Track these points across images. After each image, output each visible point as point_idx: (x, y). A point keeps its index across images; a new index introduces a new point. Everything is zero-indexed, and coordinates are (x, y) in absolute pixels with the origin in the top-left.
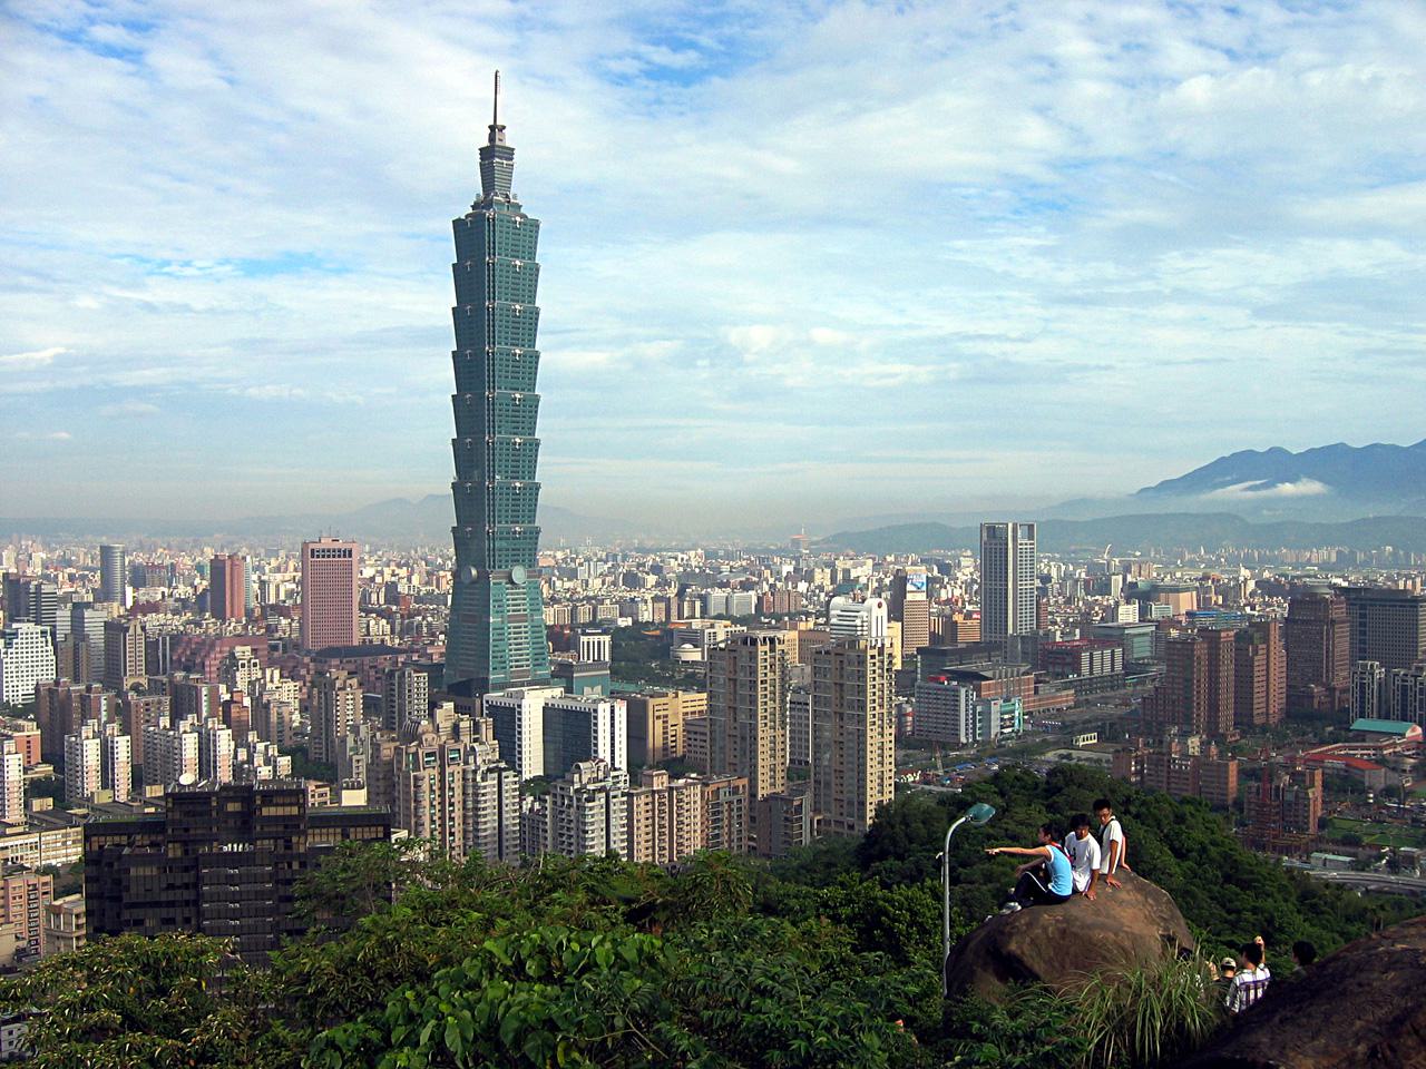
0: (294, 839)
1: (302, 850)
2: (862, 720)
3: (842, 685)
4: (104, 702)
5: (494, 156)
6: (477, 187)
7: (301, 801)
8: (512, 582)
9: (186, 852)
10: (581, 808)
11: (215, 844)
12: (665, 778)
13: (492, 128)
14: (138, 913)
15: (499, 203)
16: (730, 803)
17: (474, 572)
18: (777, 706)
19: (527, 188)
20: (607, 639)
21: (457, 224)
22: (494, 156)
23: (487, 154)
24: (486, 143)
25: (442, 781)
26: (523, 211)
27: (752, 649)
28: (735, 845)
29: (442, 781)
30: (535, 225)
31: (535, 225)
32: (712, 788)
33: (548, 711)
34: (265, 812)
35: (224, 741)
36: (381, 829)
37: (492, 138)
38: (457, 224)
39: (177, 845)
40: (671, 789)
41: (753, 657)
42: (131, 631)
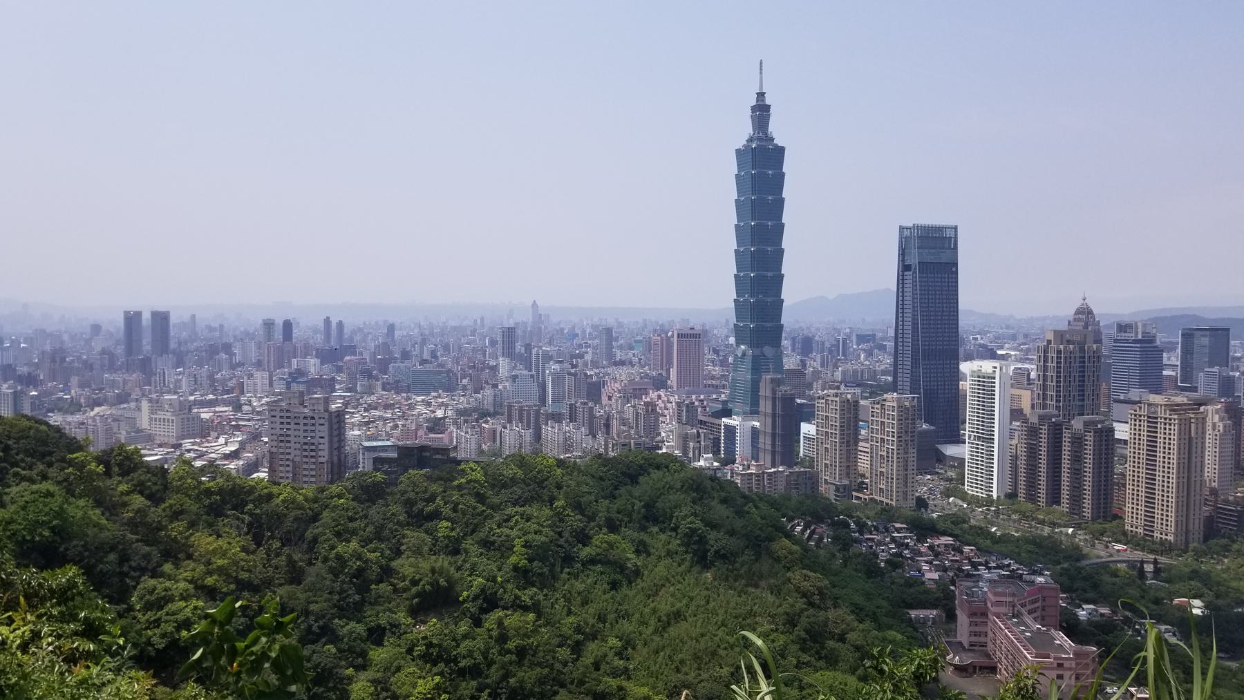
5: (761, 112)
19: (779, 131)
21: (738, 151)
22: (761, 112)
30: (781, 150)
31: (781, 150)
38: (738, 151)
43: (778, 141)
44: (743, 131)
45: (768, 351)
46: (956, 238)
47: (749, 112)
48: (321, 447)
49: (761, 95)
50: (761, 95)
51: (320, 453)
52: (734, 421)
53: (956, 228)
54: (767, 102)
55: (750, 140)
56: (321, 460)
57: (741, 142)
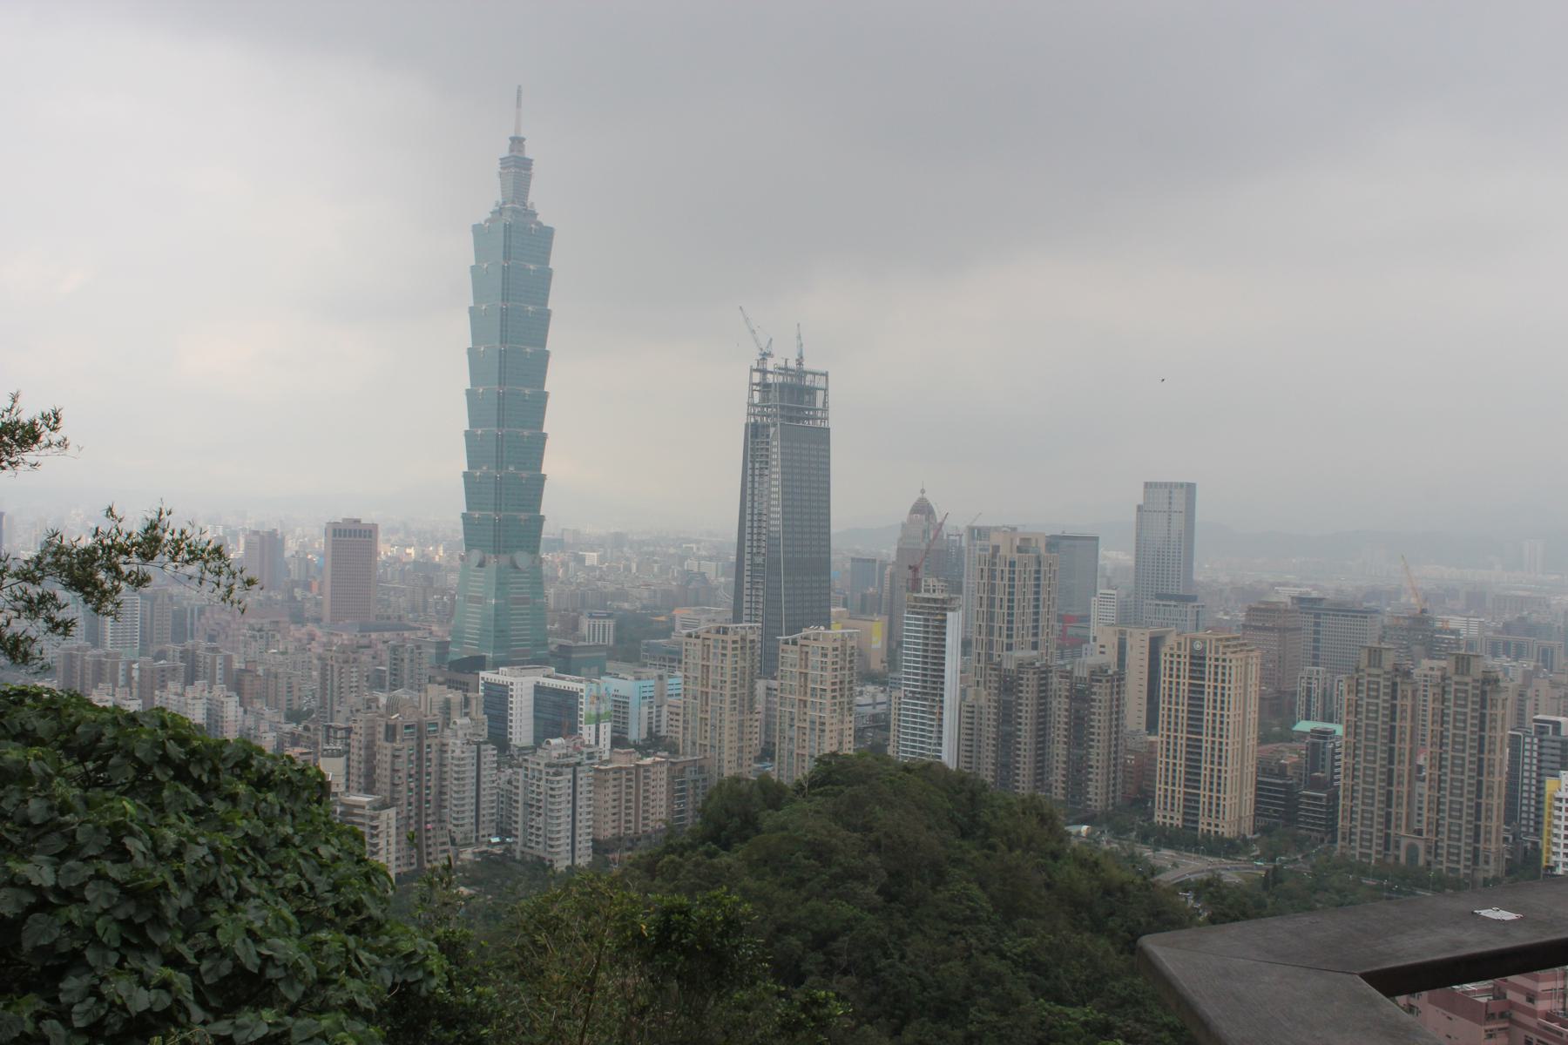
4: (121, 667)
5: (517, 168)
16: (695, 781)
18: (746, 691)
19: (545, 202)
20: (611, 623)
21: (477, 229)
24: (506, 153)
25: (420, 751)
26: (539, 218)
29: (420, 751)
31: (547, 234)
33: (539, 689)
35: (232, 709)
37: (511, 150)
38: (477, 229)
43: (545, 218)
44: (486, 197)
45: (522, 559)
46: (826, 390)
47: (497, 166)
49: (517, 142)
50: (517, 142)
52: (502, 676)
53: (826, 375)
54: (528, 154)
55: (500, 211)
57: (483, 214)
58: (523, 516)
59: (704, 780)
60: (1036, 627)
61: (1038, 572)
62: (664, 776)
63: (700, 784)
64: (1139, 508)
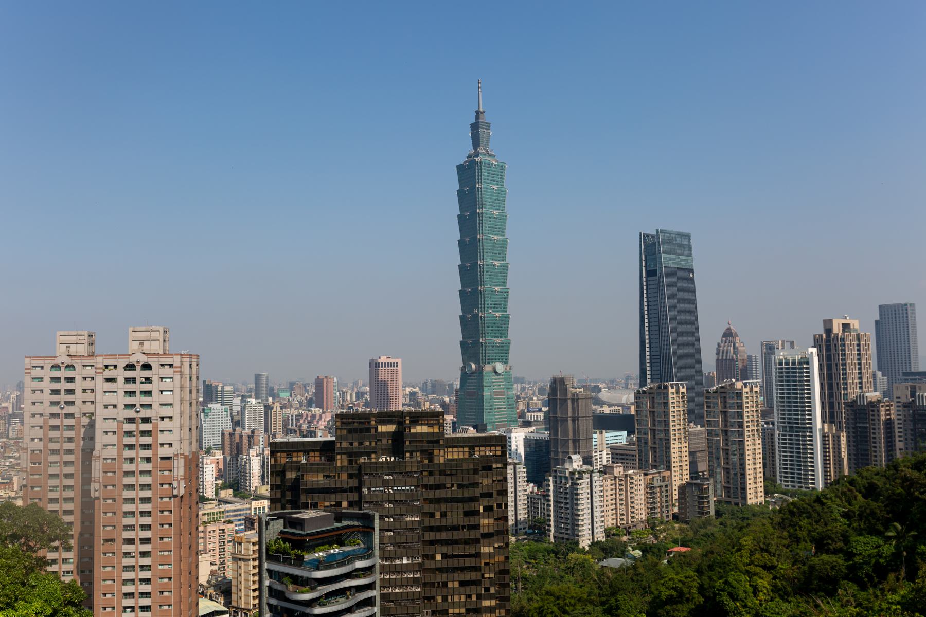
0: (436, 452)
1: (442, 460)
2: (741, 434)
3: (725, 412)
6: (469, 148)
7: (441, 421)
8: (496, 372)
9: (350, 462)
10: (575, 484)
11: (373, 456)
12: (621, 469)
13: (478, 112)
14: (316, 498)
15: (483, 154)
17: (473, 366)
21: (459, 167)
23: (475, 127)
24: (474, 121)
27: (665, 391)
28: (664, 515)
32: (650, 477)
33: (527, 441)
34: (413, 431)
36: (499, 448)
37: (477, 118)
38: (459, 167)
39: (344, 456)
40: (626, 476)
41: (666, 396)
42: (275, 409)
46: (690, 246)
48: (163, 425)
51: (162, 438)
53: (688, 236)
56: (165, 451)
57: (462, 160)
58: (498, 340)
59: (666, 486)
60: (861, 383)
61: (858, 345)
62: (642, 482)
63: (663, 489)
64: (877, 322)
